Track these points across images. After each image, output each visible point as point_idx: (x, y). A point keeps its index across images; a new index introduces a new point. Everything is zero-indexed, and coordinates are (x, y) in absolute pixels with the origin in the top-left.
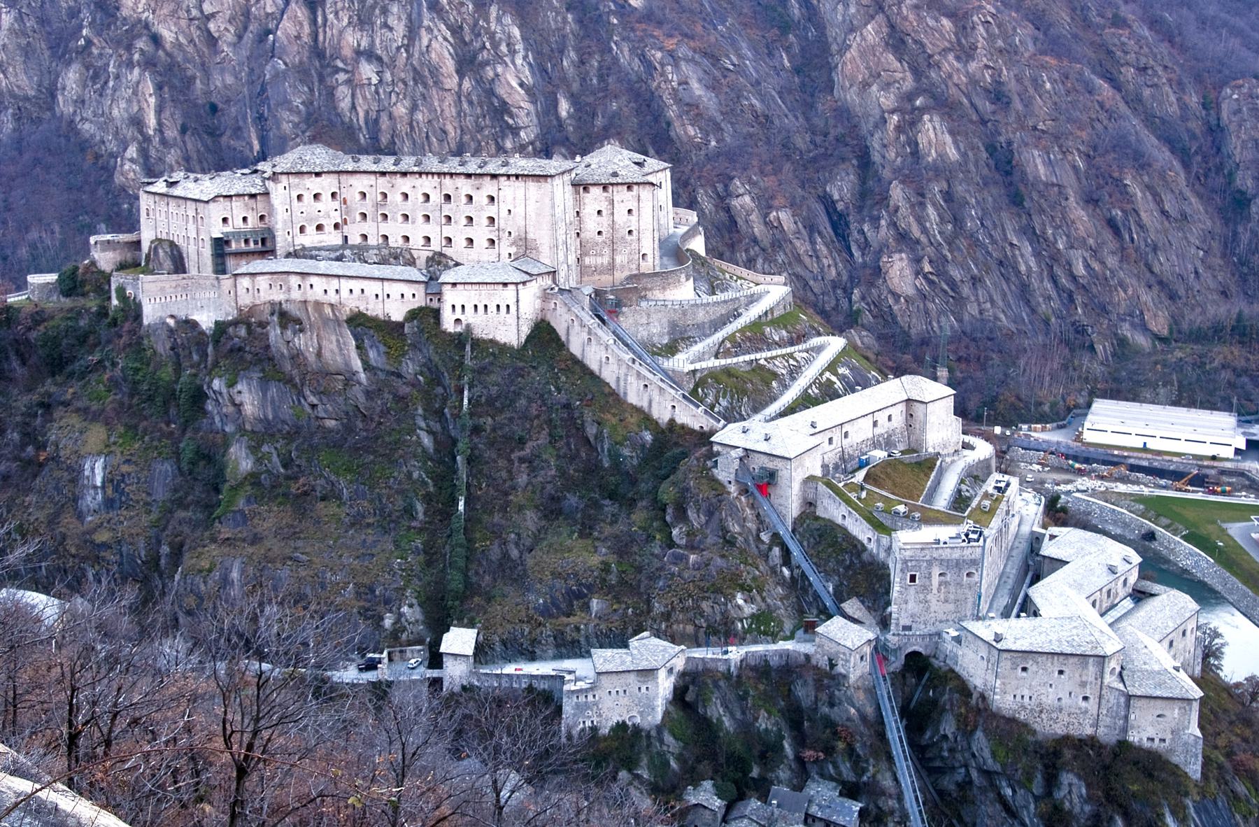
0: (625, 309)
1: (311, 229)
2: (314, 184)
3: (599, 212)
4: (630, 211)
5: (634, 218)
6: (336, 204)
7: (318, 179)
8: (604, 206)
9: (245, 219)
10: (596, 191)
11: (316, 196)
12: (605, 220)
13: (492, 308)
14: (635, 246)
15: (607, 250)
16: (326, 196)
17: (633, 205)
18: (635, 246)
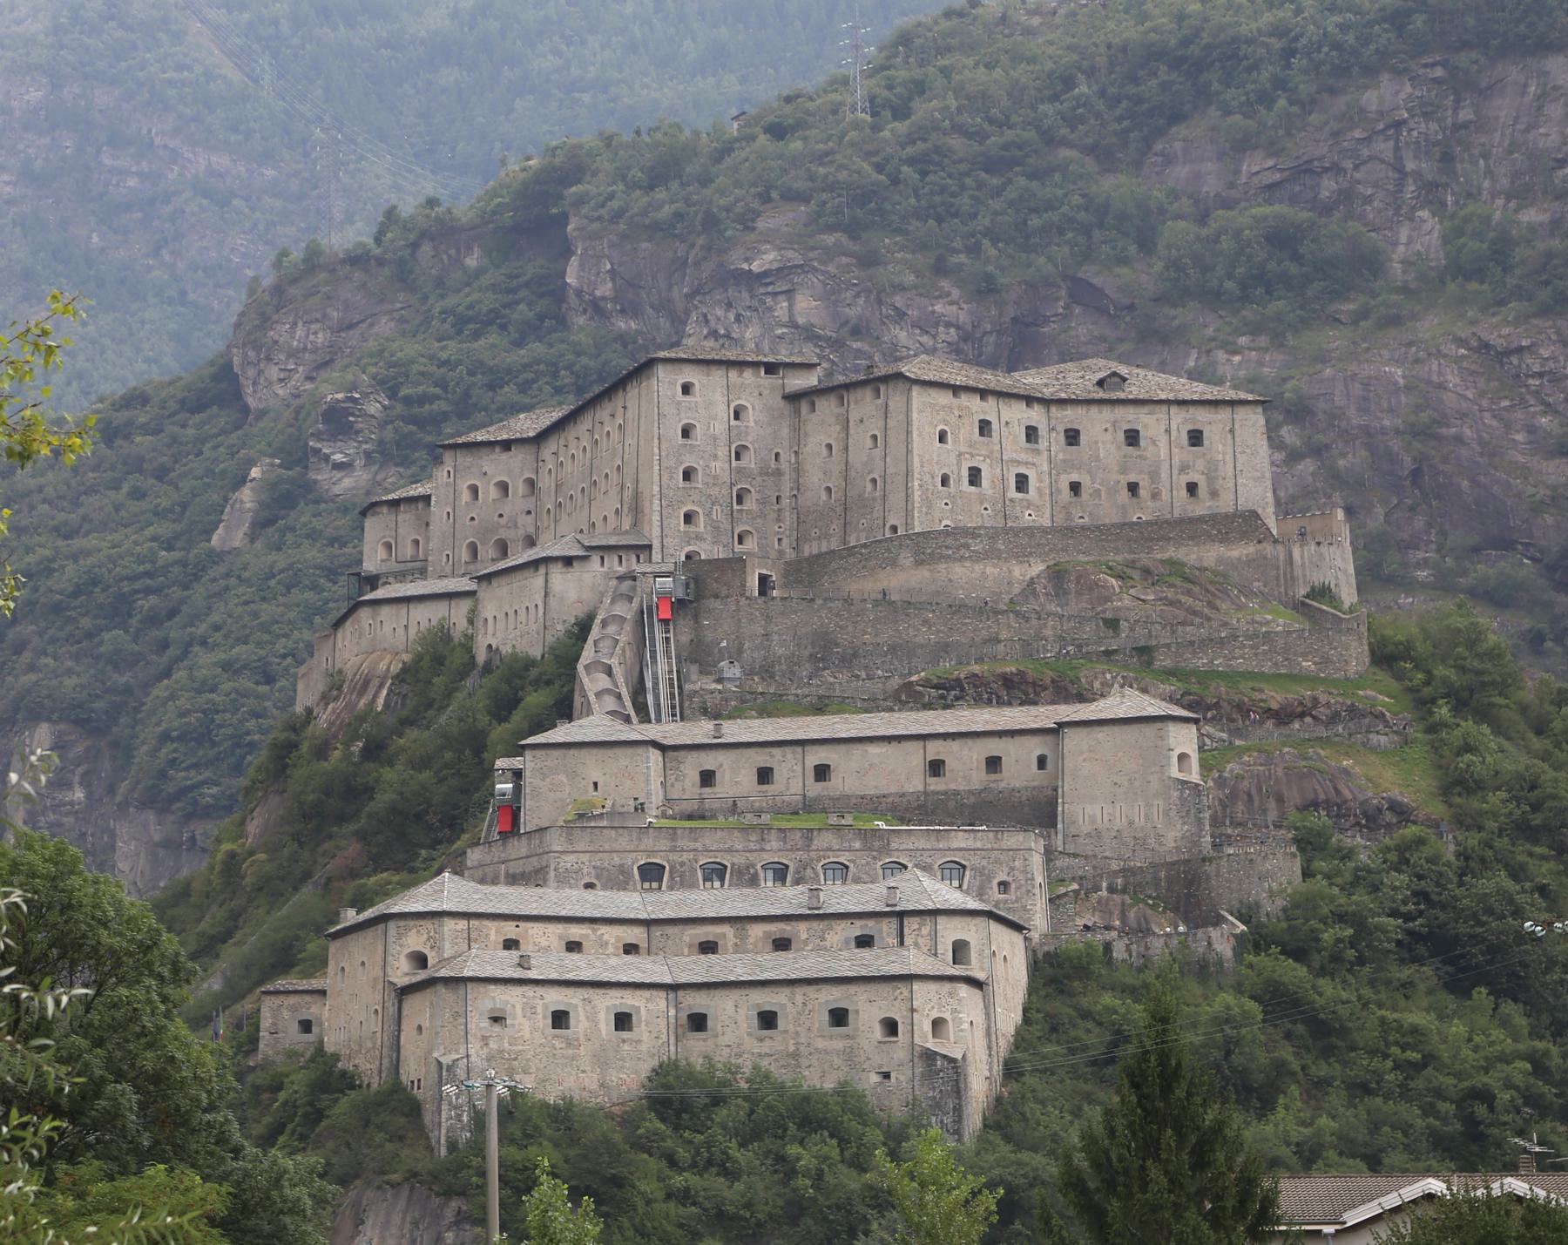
0: (716, 604)
1: (488, 552)
2: (496, 466)
3: (829, 447)
4: (874, 437)
5: (878, 452)
6: (530, 504)
7: (505, 456)
8: (833, 434)
9: (416, 542)
10: (827, 406)
11: (504, 487)
12: (836, 465)
13: (522, 613)
14: (878, 507)
15: (836, 526)
16: (518, 487)
17: (875, 427)
18: (878, 507)
